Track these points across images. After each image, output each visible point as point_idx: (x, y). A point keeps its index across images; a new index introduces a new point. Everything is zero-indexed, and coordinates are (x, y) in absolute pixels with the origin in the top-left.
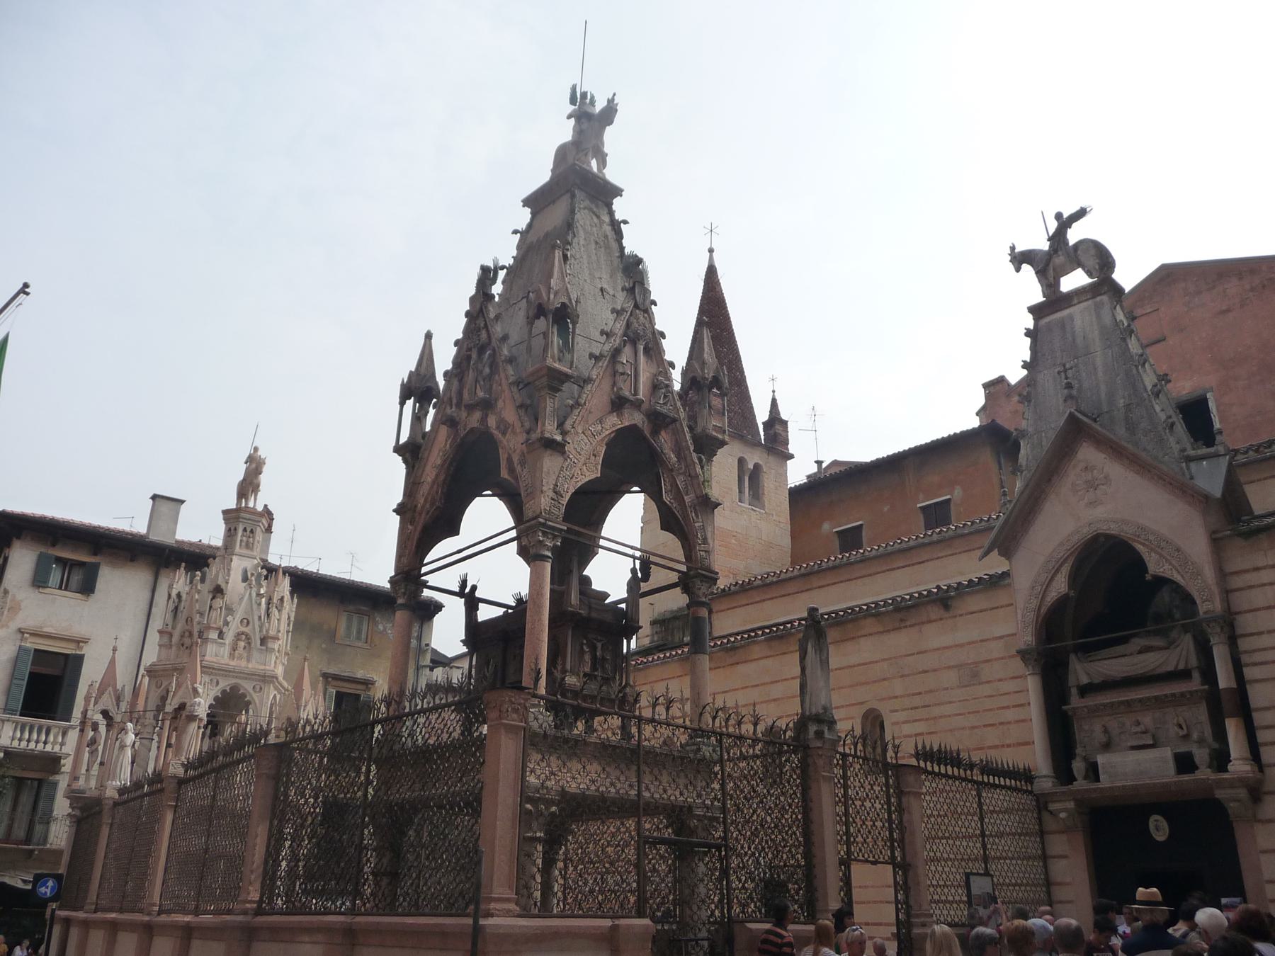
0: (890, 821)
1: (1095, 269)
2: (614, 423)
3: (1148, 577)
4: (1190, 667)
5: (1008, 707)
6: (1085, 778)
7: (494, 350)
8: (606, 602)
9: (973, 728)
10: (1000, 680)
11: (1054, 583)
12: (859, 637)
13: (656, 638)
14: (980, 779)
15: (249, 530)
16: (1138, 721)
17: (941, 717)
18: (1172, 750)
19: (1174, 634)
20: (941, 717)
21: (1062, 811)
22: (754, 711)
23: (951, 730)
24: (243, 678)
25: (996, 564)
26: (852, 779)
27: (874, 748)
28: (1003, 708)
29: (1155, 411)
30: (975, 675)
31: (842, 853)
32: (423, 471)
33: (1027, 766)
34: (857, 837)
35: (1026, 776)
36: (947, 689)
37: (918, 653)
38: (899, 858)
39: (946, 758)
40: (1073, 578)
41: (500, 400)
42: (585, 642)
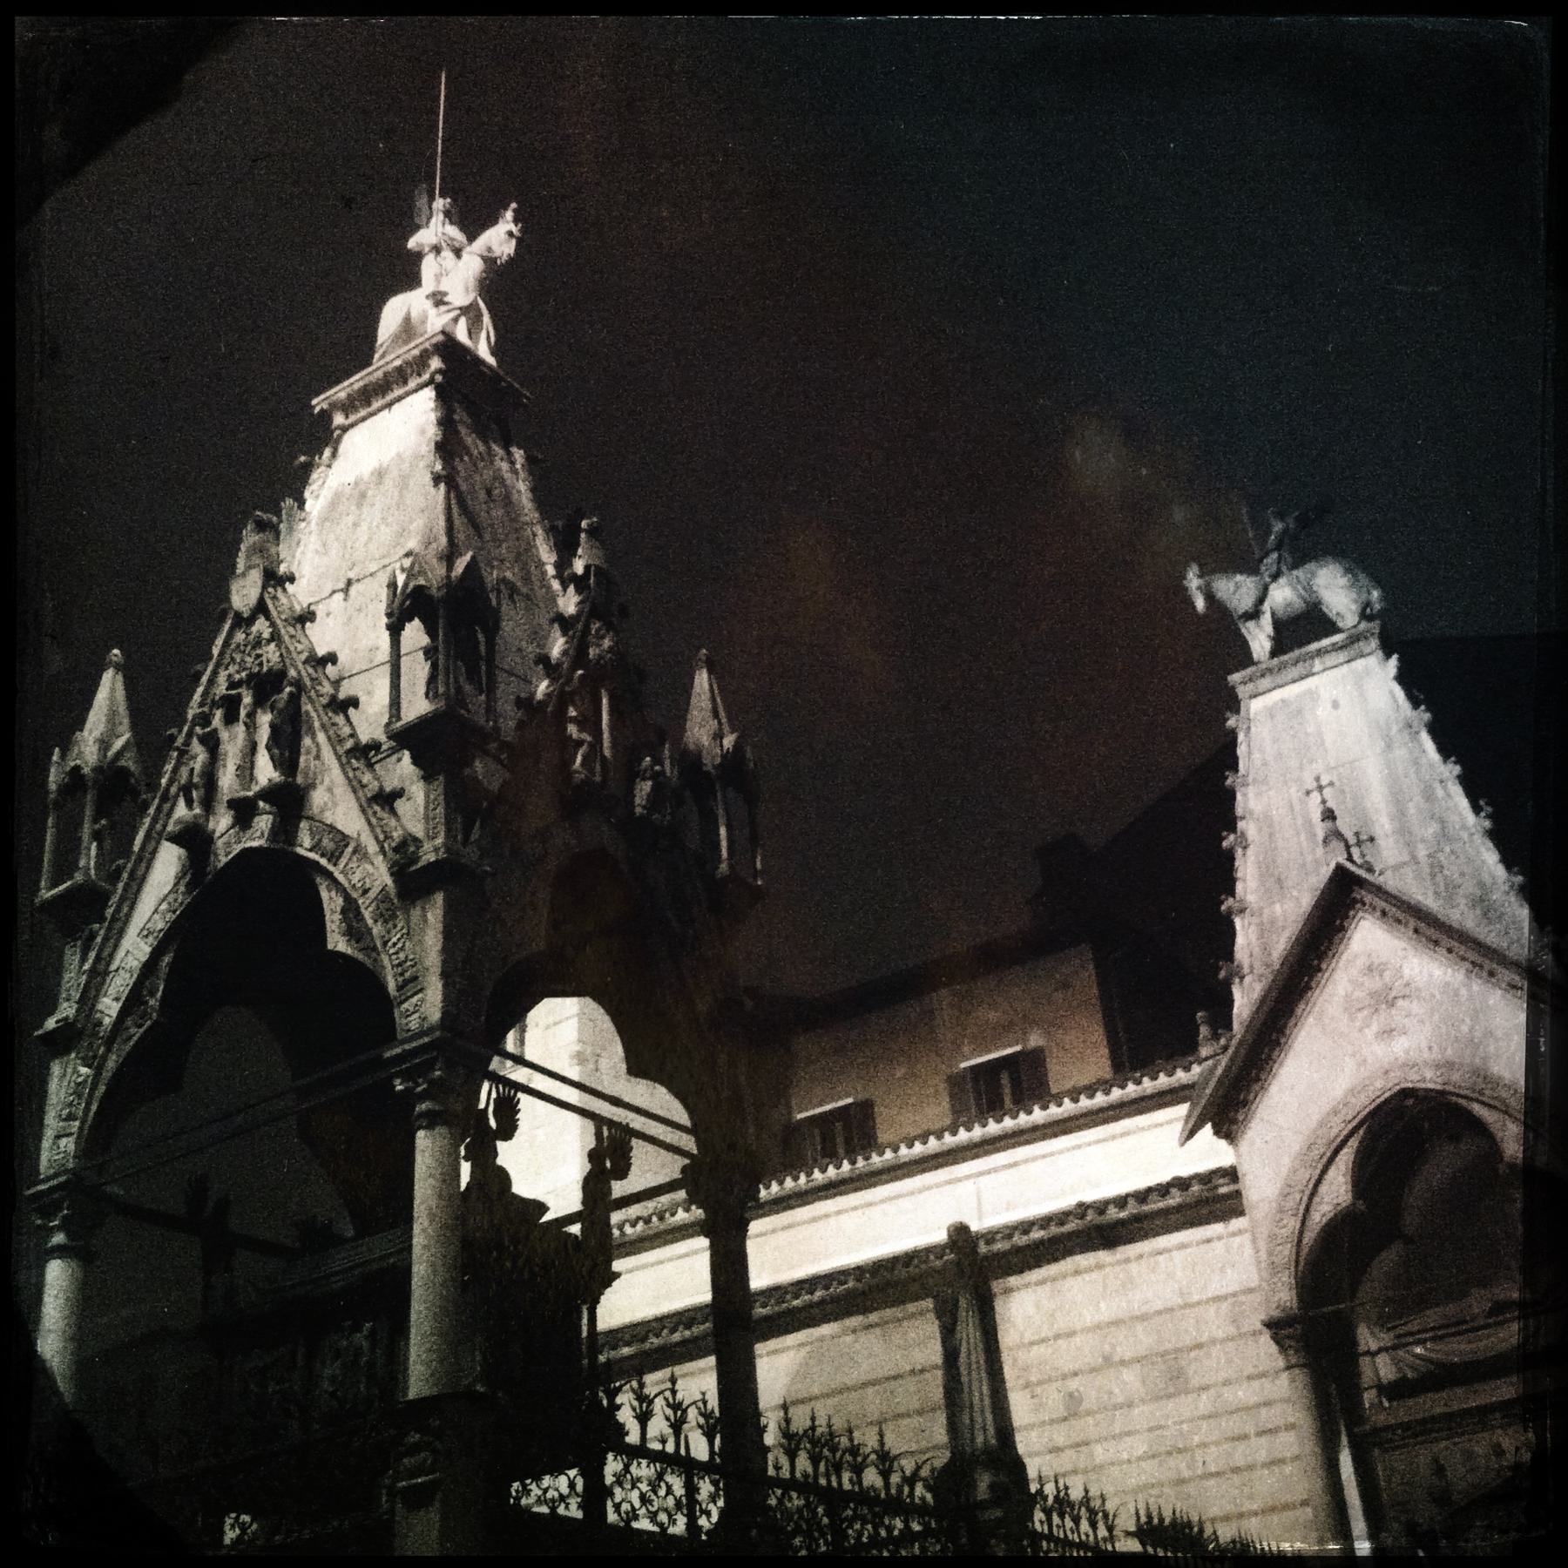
8: (544, 1219)
11: (1323, 1189)
27: (1093, 1525)
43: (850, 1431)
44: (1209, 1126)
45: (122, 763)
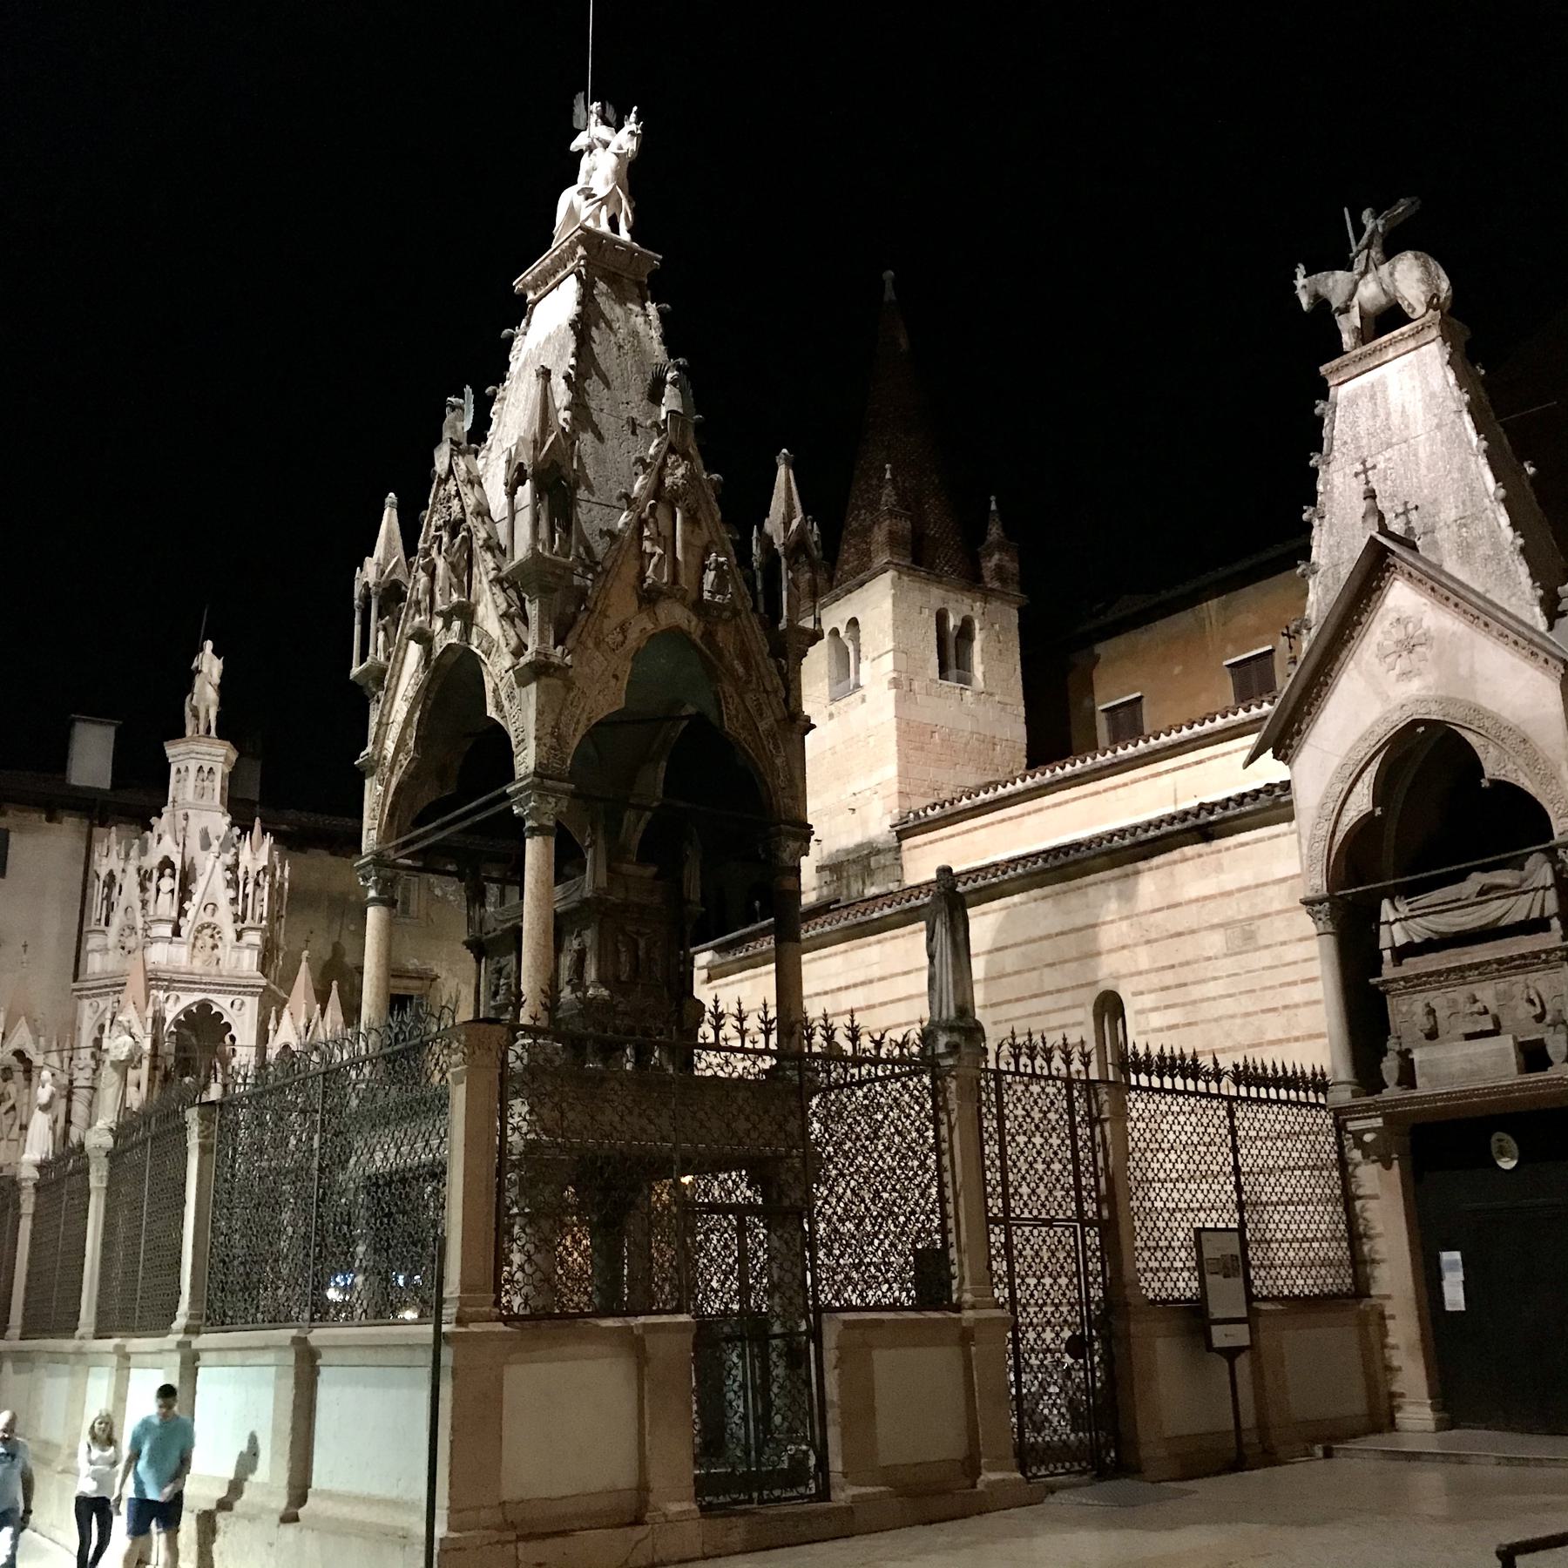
0: (1075, 1159)
1: (1419, 300)
2: (642, 626)
3: (1485, 783)
4: (1546, 914)
5: (1294, 983)
6: (1399, 1083)
7: (469, 530)
9: (1247, 1014)
10: (1283, 943)
11: (1352, 798)
12: (1087, 886)
13: (825, 891)
14: (1233, 1092)
15: (206, 769)
16: (1474, 996)
17: (1203, 1000)
18: (1515, 1038)
19: (1529, 865)
20: (1203, 1000)
21: (1368, 1131)
22: (852, 1021)
23: (1216, 1020)
24: (215, 991)
25: (1270, 770)
26: (1011, 1106)
28: (1289, 984)
29: (1499, 526)
30: (1249, 937)
31: (995, 1210)
32: (392, 706)
33: (1318, 1070)
34: (1020, 1186)
35: (1319, 1083)
36: (1209, 959)
37: (1169, 907)
38: (1090, 1214)
39: (1173, 1066)
40: (1381, 793)
41: (482, 605)
42: (620, 937)
43: (852, 1012)
44: (1270, 752)
45: (394, 577)
